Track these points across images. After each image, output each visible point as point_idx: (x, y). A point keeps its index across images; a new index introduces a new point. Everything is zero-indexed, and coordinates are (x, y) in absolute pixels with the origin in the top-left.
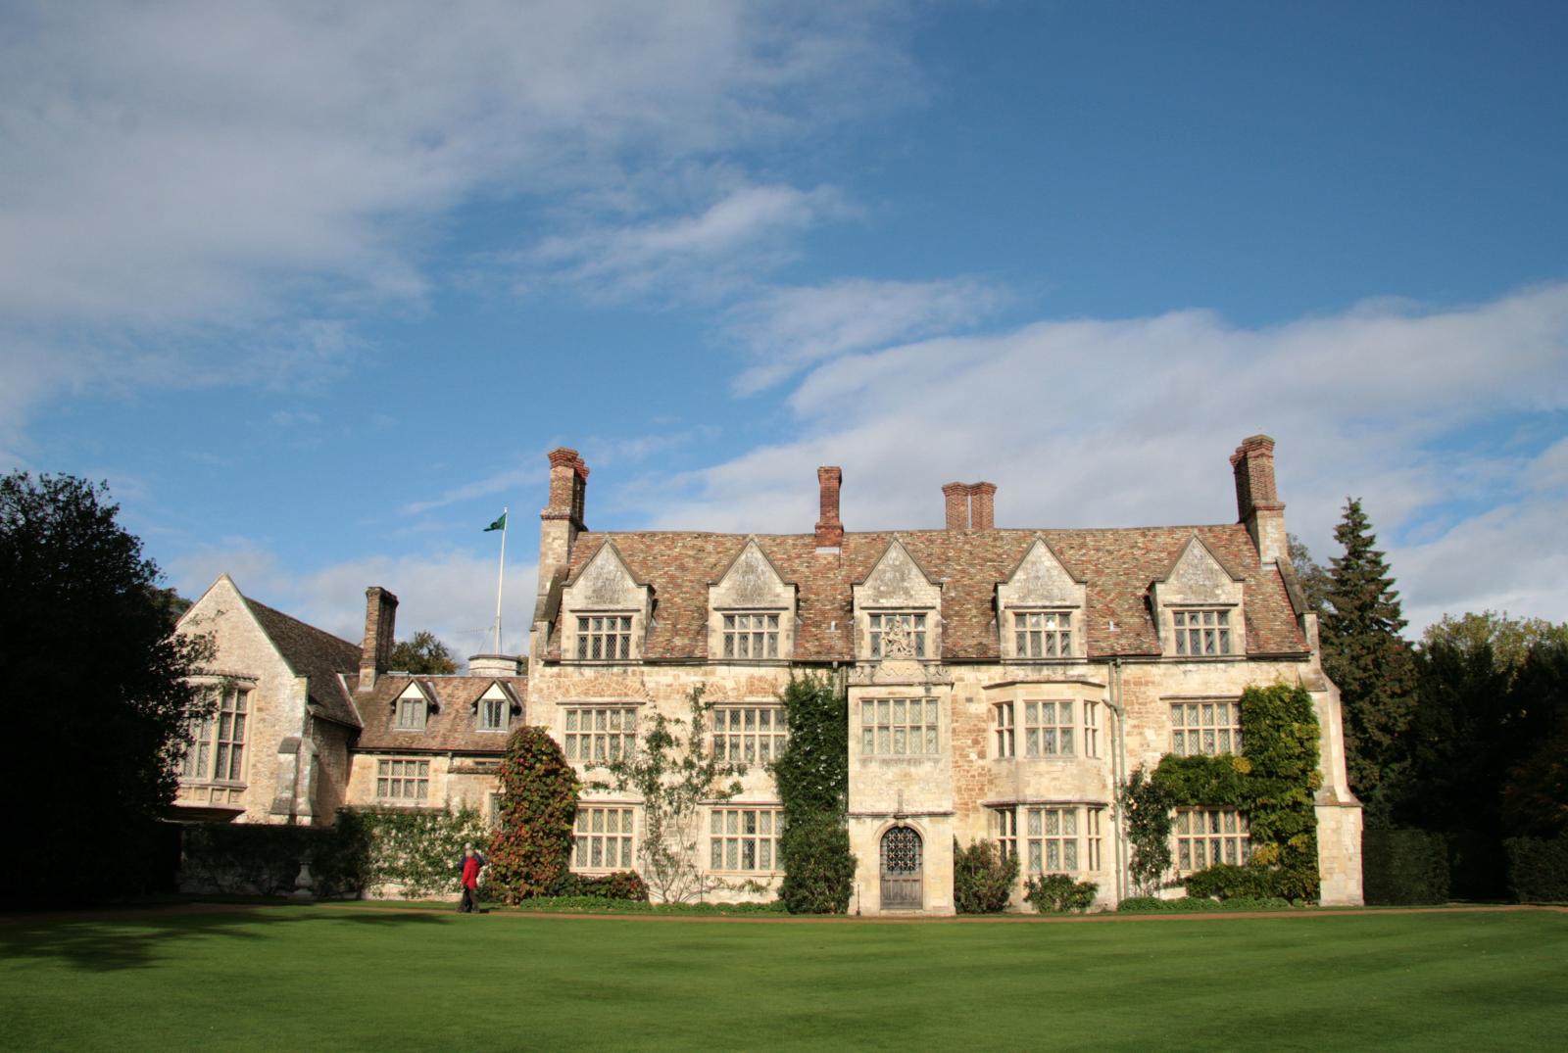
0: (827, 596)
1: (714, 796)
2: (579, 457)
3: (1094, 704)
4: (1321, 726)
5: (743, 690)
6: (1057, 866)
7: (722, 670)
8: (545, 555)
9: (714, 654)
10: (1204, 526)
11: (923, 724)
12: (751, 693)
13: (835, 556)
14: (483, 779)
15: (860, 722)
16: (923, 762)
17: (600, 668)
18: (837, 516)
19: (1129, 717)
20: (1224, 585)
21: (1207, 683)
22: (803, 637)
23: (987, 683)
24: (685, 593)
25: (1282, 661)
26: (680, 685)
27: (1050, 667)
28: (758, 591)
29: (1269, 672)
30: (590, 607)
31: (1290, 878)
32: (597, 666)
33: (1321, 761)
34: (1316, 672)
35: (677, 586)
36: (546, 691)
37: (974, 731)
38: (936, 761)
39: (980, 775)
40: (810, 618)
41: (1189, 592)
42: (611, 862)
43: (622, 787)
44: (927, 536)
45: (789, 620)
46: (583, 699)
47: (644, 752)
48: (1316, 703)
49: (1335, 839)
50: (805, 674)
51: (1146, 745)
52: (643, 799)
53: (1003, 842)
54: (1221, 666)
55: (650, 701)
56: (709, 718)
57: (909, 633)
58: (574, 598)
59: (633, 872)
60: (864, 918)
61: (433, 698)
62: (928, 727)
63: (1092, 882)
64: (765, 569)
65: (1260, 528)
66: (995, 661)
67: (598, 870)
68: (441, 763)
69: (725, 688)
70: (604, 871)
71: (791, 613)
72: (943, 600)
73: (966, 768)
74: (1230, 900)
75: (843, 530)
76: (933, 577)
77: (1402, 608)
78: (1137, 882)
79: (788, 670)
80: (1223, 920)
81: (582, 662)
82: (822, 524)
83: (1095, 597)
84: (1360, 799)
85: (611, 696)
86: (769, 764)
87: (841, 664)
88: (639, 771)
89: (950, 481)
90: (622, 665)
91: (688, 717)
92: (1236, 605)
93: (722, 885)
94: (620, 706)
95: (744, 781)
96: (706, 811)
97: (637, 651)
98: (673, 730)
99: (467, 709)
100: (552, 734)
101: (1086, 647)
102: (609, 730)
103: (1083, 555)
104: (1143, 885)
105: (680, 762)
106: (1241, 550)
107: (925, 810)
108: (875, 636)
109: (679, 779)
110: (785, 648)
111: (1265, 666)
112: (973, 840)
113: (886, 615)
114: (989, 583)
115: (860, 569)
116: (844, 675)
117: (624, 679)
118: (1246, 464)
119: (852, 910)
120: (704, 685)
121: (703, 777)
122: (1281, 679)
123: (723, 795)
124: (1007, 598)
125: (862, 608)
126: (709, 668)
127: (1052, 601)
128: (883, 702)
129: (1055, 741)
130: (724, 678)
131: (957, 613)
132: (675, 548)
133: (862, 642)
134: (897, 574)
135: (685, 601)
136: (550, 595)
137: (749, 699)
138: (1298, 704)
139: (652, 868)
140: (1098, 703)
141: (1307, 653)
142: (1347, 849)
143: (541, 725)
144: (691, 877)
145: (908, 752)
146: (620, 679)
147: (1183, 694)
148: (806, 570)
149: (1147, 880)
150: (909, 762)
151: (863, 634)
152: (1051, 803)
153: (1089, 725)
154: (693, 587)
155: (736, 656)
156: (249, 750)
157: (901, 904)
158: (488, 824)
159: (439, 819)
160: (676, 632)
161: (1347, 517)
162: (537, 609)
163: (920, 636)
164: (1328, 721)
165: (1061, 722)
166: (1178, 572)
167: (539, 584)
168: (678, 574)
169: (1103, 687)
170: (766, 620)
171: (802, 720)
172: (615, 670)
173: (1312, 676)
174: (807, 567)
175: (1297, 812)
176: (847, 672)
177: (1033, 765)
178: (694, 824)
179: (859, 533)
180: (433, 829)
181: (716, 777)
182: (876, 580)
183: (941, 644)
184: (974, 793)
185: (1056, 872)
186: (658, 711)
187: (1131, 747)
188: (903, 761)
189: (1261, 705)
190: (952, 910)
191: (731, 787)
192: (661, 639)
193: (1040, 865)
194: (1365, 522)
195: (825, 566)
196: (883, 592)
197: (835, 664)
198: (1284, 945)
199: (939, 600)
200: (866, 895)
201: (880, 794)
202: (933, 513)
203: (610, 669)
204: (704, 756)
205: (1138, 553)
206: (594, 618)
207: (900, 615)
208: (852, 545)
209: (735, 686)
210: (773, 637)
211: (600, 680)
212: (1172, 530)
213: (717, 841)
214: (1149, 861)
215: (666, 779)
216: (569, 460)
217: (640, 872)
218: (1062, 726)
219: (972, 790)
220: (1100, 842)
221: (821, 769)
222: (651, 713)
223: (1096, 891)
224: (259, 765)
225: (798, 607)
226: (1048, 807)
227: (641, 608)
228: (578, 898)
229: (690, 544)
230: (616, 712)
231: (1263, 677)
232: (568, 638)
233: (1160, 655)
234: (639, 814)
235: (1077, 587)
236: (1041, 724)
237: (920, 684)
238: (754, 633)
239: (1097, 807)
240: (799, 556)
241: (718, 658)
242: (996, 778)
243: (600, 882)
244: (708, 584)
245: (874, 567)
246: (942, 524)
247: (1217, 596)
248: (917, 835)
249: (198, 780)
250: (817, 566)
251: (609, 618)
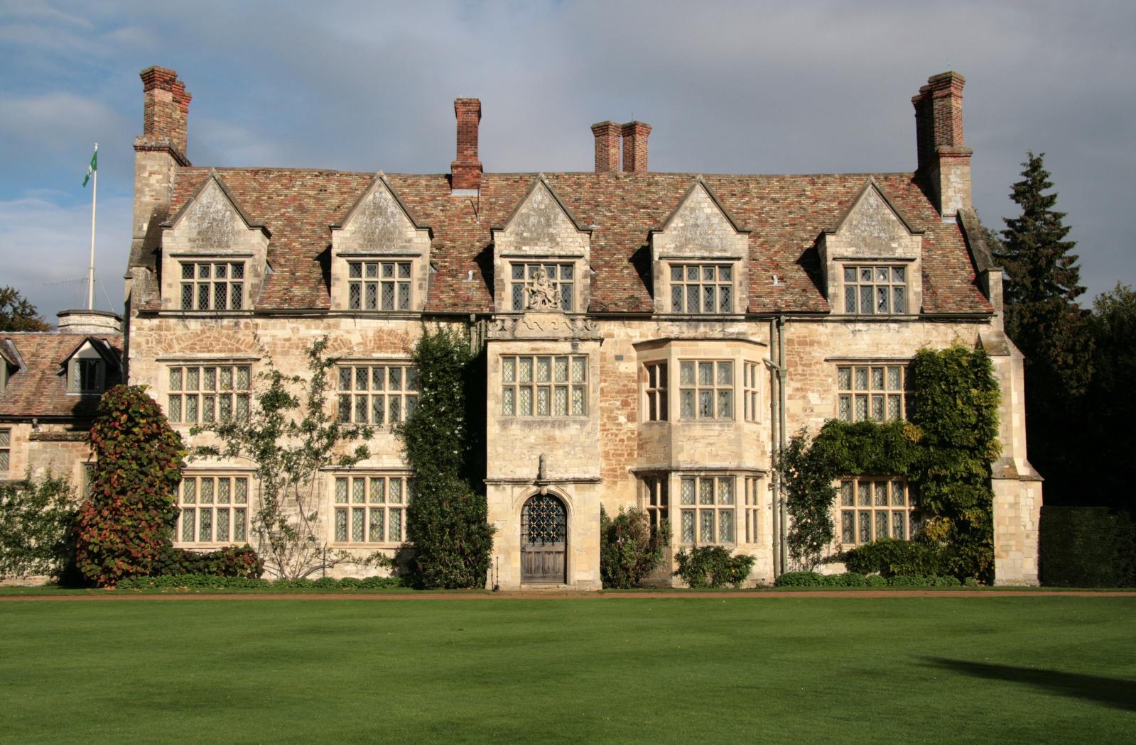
0: (463, 243)
1: (339, 461)
2: (178, 79)
3: (754, 365)
4: (1001, 389)
5: (371, 345)
6: (712, 539)
7: (347, 323)
8: (141, 192)
9: (338, 305)
10: (879, 174)
11: (570, 383)
12: (380, 348)
13: (470, 199)
14: (73, 446)
15: (500, 379)
16: (569, 424)
17: (208, 320)
18: (476, 154)
19: (792, 379)
20: (901, 237)
21: (878, 344)
22: (437, 288)
23: (638, 340)
24: (303, 237)
25: (961, 322)
26: (300, 339)
27: (708, 324)
28: (387, 236)
29: (946, 334)
30: (195, 251)
31: (961, 556)
32: (204, 317)
33: (1000, 429)
34: (999, 335)
35: (295, 230)
36: (144, 346)
37: (624, 392)
38: (583, 424)
39: (629, 439)
40: (445, 266)
41: (862, 244)
42: (224, 535)
43: (233, 452)
44: (576, 179)
45: (423, 268)
46: (188, 355)
47: (260, 413)
48: (998, 368)
49: (1013, 515)
50: (439, 327)
51: (809, 410)
52: (258, 465)
53: (653, 512)
54: (893, 325)
55: (265, 357)
56: (333, 376)
57: (555, 285)
58: (175, 241)
59: (247, 546)
60: (503, 593)
61: (13, 357)
62: (574, 386)
63: (749, 556)
64: (395, 212)
65: (942, 176)
66: (646, 317)
67: (208, 544)
68: (24, 430)
69: (350, 343)
70: (215, 545)
71: (426, 259)
72: (592, 249)
73: (614, 431)
74: (896, 577)
75: (482, 170)
76: (581, 224)
77: (1080, 273)
78: (796, 555)
79: (420, 323)
80: (896, 599)
81: (186, 314)
82: (458, 163)
83: (758, 249)
84: (1042, 475)
85: (220, 351)
86: (398, 427)
87: (479, 317)
88: (251, 434)
89: (600, 120)
90: (234, 317)
91: (309, 375)
92: (912, 260)
93: (347, 558)
94: (231, 362)
95: (371, 444)
96: (330, 478)
97: (250, 301)
98: (291, 389)
99: (55, 369)
100: (152, 394)
101: (747, 303)
102: (219, 389)
103: (744, 204)
104: (803, 559)
105: (299, 423)
106: (920, 201)
107: (570, 476)
108: (517, 289)
109: (298, 442)
110: (418, 299)
111: (942, 327)
112: (621, 509)
113: (529, 264)
114: (642, 232)
115: (500, 214)
116: (483, 330)
117: (235, 332)
118: (932, 105)
119: (489, 586)
120: (326, 338)
121: (325, 441)
122: (959, 342)
123: (347, 461)
124: (663, 248)
125: (502, 256)
126: (332, 321)
127: (711, 251)
128: (527, 358)
129: (716, 403)
130: (348, 332)
131: (607, 264)
132: (294, 187)
133: (503, 293)
134: (542, 219)
135: (305, 246)
136: (147, 238)
137: (375, 355)
138: (976, 366)
139: (268, 541)
140: (759, 363)
141: (990, 313)
142: (1025, 526)
143: (140, 383)
144: (312, 551)
145: (553, 413)
146: (231, 332)
147: (851, 356)
148: (441, 214)
149: (807, 554)
150: (553, 424)
151: (504, 285)
152: (706, 470)
153: (749, 387)
154: (313, 231)
155: (363, 307)
157: (544, 577)
158: (79, 497)
159: (19, 493)
160: (294, 280)
161: (1026, 174)
162: (133, 254)
163: (567, 289)
164: (1010, 388)
165: (719, 383)
166: (851, 222)
167: (135, 225)
168: (296, 216)
169: (765, 345)
170: (396, 267)
171: (435, 379)
172: (225, 322)
173: (994, 339)
174: (442, 210)
175: (971, 484)
176: (486, 327)
177: (687, 429)
178: (315, 492)
179: (500, 175)
180: (10, 505)
181: (340, 442)
182: (519, 225)
183: (590, 297)
184: (623, 459)
185: (711, 544)
186: (275, 368)
187: (792, 411)
188: (547, 423)
189: (938, 369)
190: (598, 584)
191: (356, 452)
192: (277, 288)
193: (694, 540)
194: (1046, 180)
195: (462, 210)
196: (524, 239)
197: (473, 318)
198: (982, 630)
199: (588, 249)
200: (506, 566)
201: (521, 458)
202: (579, 156)
203: (219, 320)
204: (326, 417)
205: (806, 202)
206: (200, 263)
207: (546, 264)
208: (492, 188)
209: (361, 340)
210: (405, 287)
211: (208, 334)
212: (843, 178)
213: (342, 511)
214: (808, 532)
215: (282, 442)
216: (165, 81)
217: (255, 545)
218: (719, 387)
219: (622, 455)
220: (758, 512)
221: (456, 432)
222: (266, 370)
223: (753, 564)
225: (433, 255)
226: (703, 474)
227: (254, 252)
228: (184, 577)
229: (310, 183)
230: (227, 369)
231: (940, 339)
232: (170, 285)
233: (829, 312)
234: (253, 483)
235: (739, 236)
236: (697, 386)
237: (566, 339)
238: (383, 282)
239: (757, 475)
240: (434, 199)
241: (342, 309)
242: (647, 443)
243: (207, 558)
244: (330, 227)
245: (516, 210)
246: (591, 167)
247: (893, 250)
248: (562, 504)
250: (452, 209)
251: (217, 263)
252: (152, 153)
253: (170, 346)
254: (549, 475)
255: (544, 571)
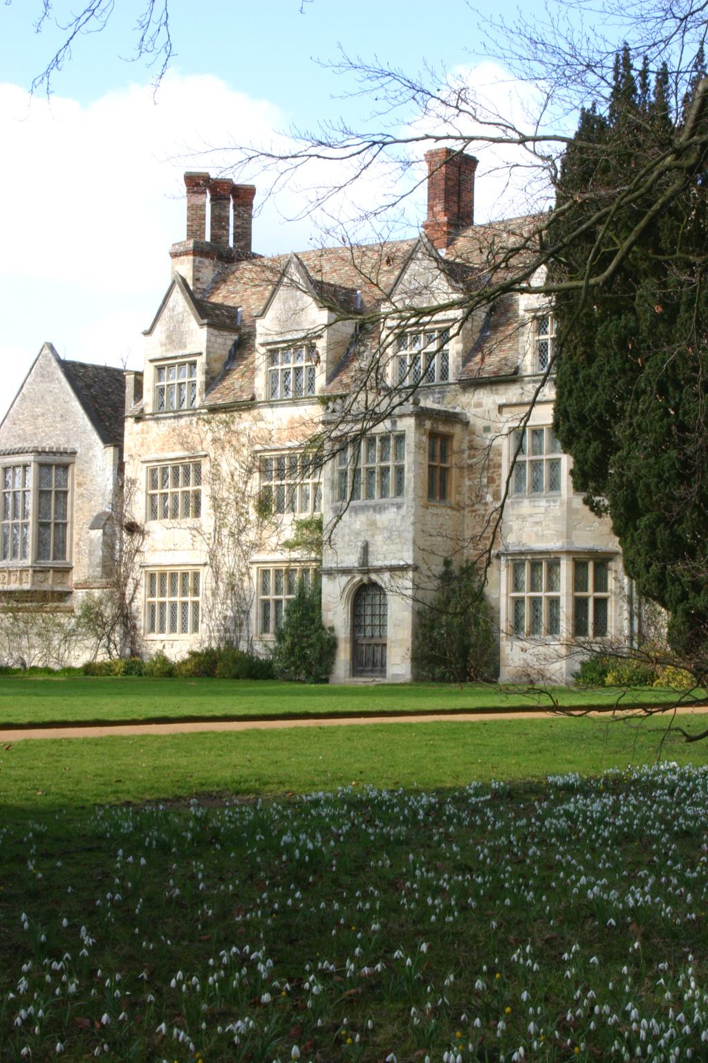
7: (266, 412)
9: (260, 395)
38: (399, 506)
94: (187, 460)
107: (387, 563)
156: (72, 527)
157: (372, 671)
224: (81, 543)
249: (20, 563)
252: (182, 258)
253: (149, 448)
254: (376, 562)
255: (374, 665)
